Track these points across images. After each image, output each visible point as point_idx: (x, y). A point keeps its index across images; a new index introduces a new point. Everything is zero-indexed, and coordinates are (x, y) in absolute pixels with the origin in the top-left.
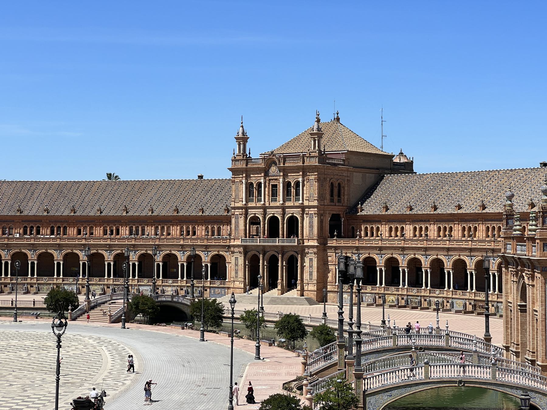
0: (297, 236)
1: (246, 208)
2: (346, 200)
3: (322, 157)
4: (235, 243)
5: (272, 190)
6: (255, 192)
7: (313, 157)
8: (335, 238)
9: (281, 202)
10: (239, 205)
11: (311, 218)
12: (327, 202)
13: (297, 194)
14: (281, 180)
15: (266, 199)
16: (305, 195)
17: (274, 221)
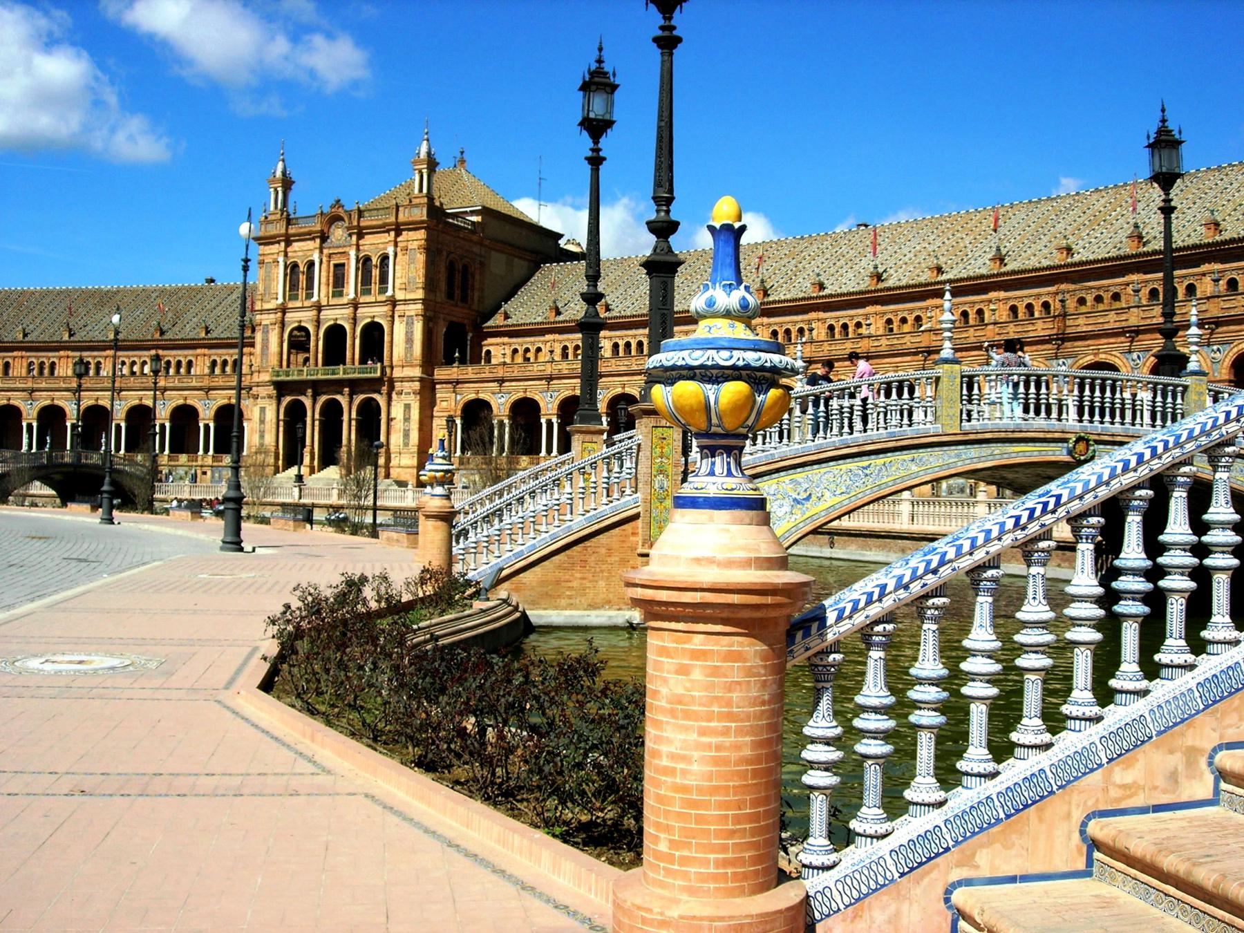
0: (381, 360)
1: (284, 310)
2: (476, 299)
3: (436, 213)
4: (261, 379)
5: (335, 275)
6: (303, 279)
7: (417, 206)
8: (456, 364)
9: (352, 296)
10: (272, 305)
11: (410, 324)
12: (441, 296)
13: (383, 279)
14: (353, 253)
15: (321, 292)
16: (398, 282)
17: (336, 335)
